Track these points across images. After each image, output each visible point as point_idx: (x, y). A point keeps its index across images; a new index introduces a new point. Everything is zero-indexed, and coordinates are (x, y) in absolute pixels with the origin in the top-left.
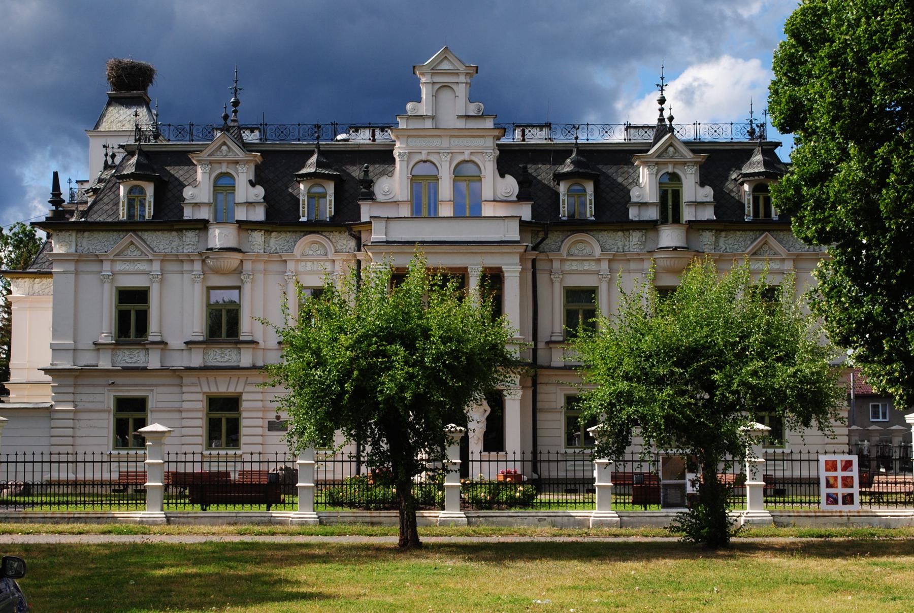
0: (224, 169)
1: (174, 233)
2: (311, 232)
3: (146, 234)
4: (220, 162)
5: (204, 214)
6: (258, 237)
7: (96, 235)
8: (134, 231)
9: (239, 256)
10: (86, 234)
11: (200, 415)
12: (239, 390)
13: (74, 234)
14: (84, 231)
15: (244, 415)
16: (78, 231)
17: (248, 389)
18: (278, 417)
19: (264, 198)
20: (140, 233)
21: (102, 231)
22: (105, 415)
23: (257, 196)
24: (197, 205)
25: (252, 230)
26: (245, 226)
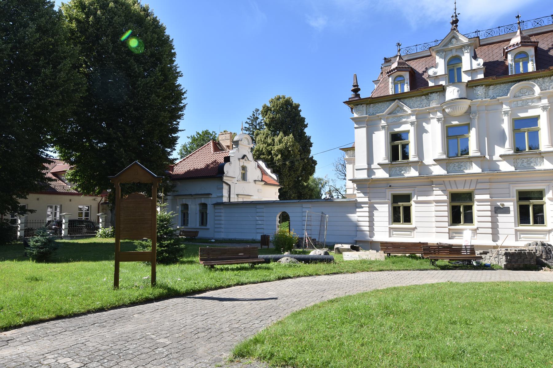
0: (454, 53)
1: (424, 97)
2: (519, 81)
3: (406, 100)
4: (451, 50)
5: (443, 83)
6: (480, 91)
7: (377, 105)
8: (399, 99)
9: (468, 102)
10: (372, 105)
11: (446, 204)
12: (472, 188)
13: (365, 106)
14: (370, 104)
15: (476, 203)
16: (367, 104)
17: (479, 186)
18: (503, 205)
19: (484, 65)
20: (402, 100)
21: (380, 102)
22: (387, 205)
23: (479, 65)
24: (436, 78)
25: (476, 86)
26: (472, 85)
